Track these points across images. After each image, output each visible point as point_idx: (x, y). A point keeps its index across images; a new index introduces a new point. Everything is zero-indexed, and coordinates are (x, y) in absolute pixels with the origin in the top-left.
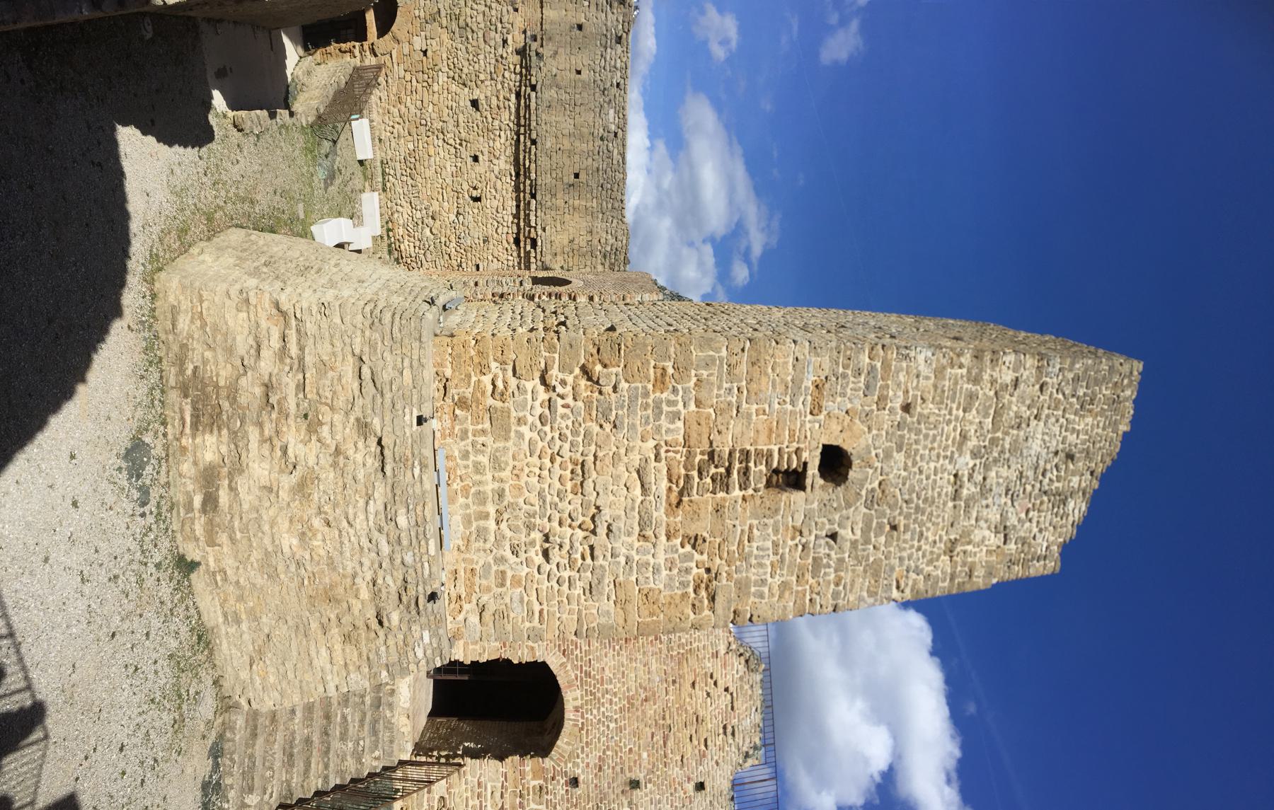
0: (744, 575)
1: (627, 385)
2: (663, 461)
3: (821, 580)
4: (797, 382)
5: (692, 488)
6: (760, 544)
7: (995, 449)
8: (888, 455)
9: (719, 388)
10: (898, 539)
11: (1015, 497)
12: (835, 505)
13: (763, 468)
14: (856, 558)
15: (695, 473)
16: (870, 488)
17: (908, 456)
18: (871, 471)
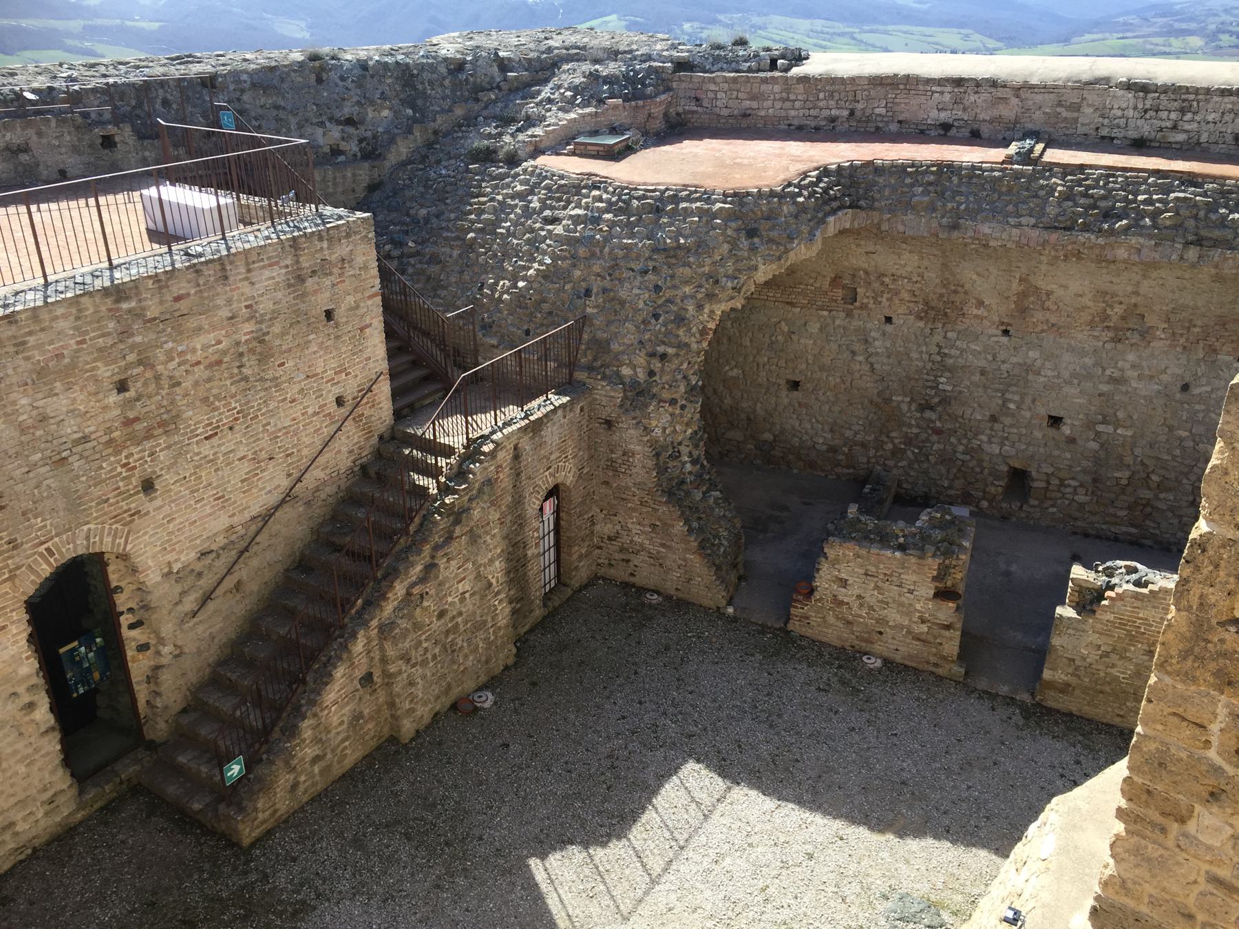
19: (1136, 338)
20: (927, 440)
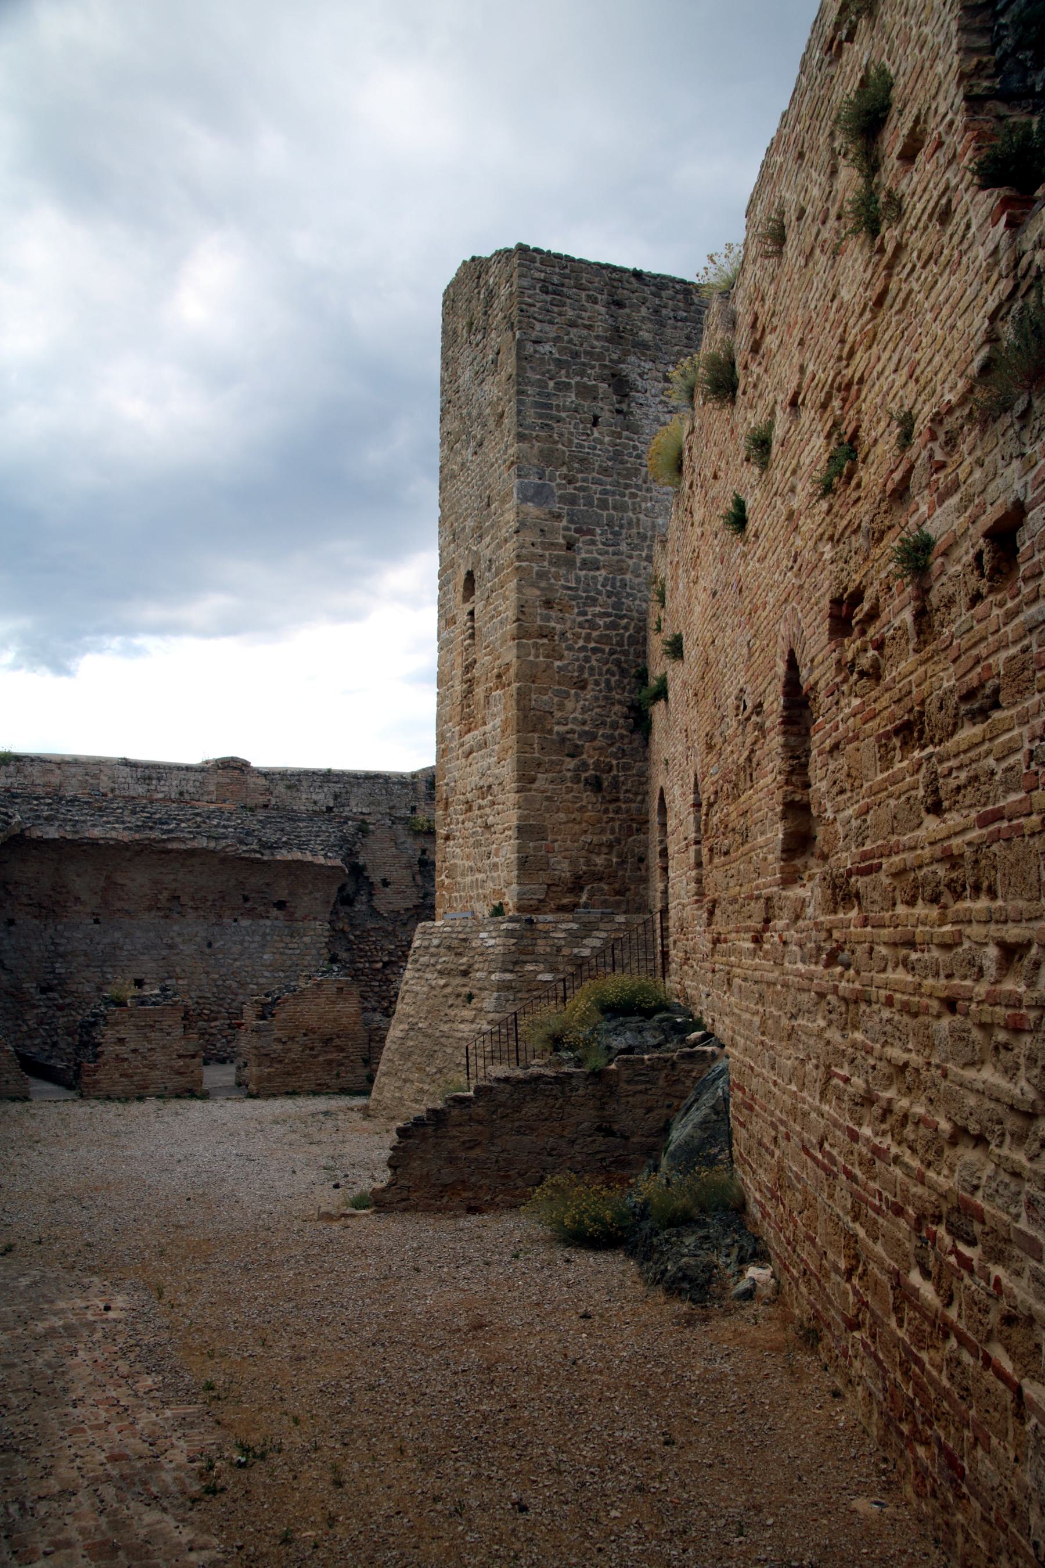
19: (176, 916)
20: (54, 1016)
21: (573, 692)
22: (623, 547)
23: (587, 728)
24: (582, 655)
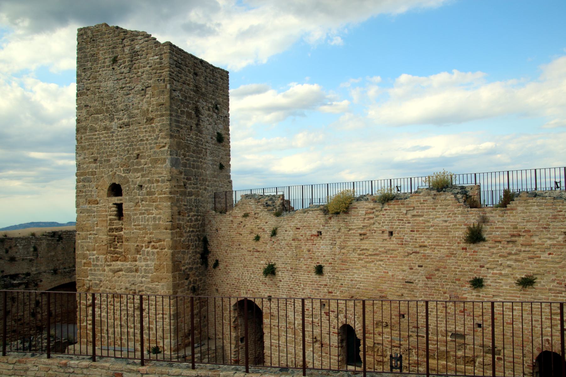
0: (151, 227)
1: (89, 277)
2: (111, 263)
3: (156, 190)
4: (88, 211)
5: (120, 252)
6: (140, 220)
7: (111, 109)
8: (111, 166)
9: (89, 242)
10: (143, 152)
11: (131, 89)
12: (127, 188)
13: (115, 222)
14: (148, 173)
15: (117, 250)
16: (122, 172)
17: (112, 156)
18: (117, 173)
21: (187, 251)
22: (199, 185)
23: (190, 266)
24: (189, 234)
